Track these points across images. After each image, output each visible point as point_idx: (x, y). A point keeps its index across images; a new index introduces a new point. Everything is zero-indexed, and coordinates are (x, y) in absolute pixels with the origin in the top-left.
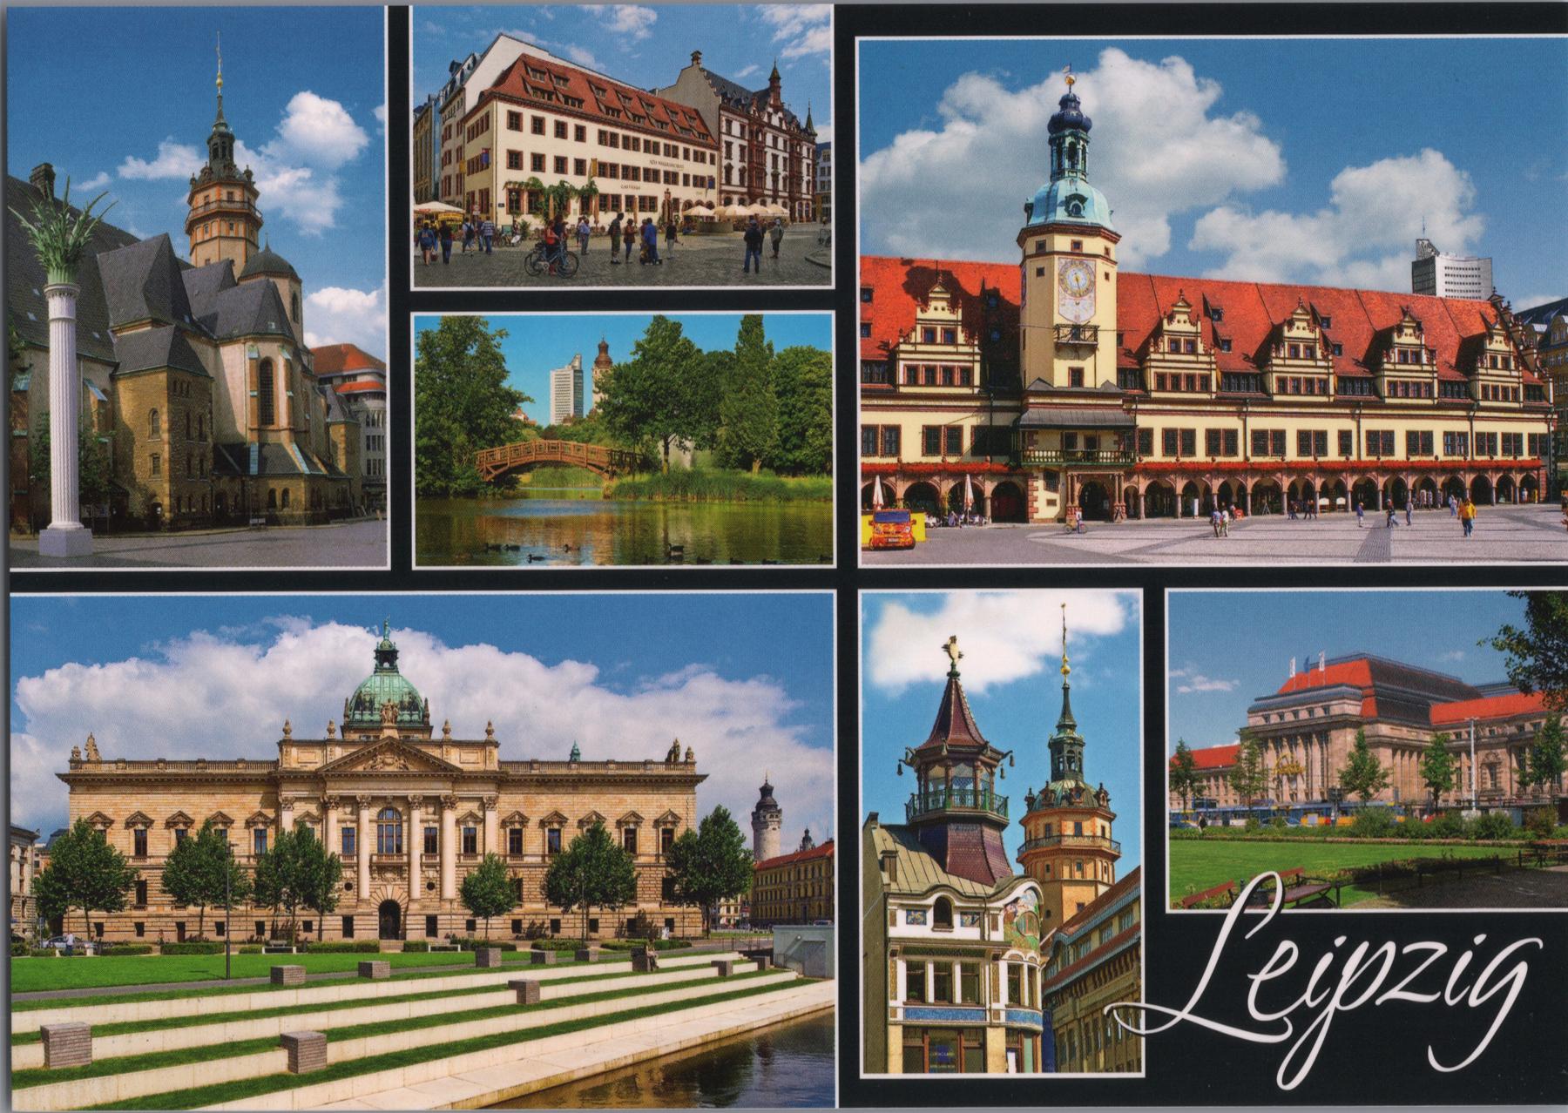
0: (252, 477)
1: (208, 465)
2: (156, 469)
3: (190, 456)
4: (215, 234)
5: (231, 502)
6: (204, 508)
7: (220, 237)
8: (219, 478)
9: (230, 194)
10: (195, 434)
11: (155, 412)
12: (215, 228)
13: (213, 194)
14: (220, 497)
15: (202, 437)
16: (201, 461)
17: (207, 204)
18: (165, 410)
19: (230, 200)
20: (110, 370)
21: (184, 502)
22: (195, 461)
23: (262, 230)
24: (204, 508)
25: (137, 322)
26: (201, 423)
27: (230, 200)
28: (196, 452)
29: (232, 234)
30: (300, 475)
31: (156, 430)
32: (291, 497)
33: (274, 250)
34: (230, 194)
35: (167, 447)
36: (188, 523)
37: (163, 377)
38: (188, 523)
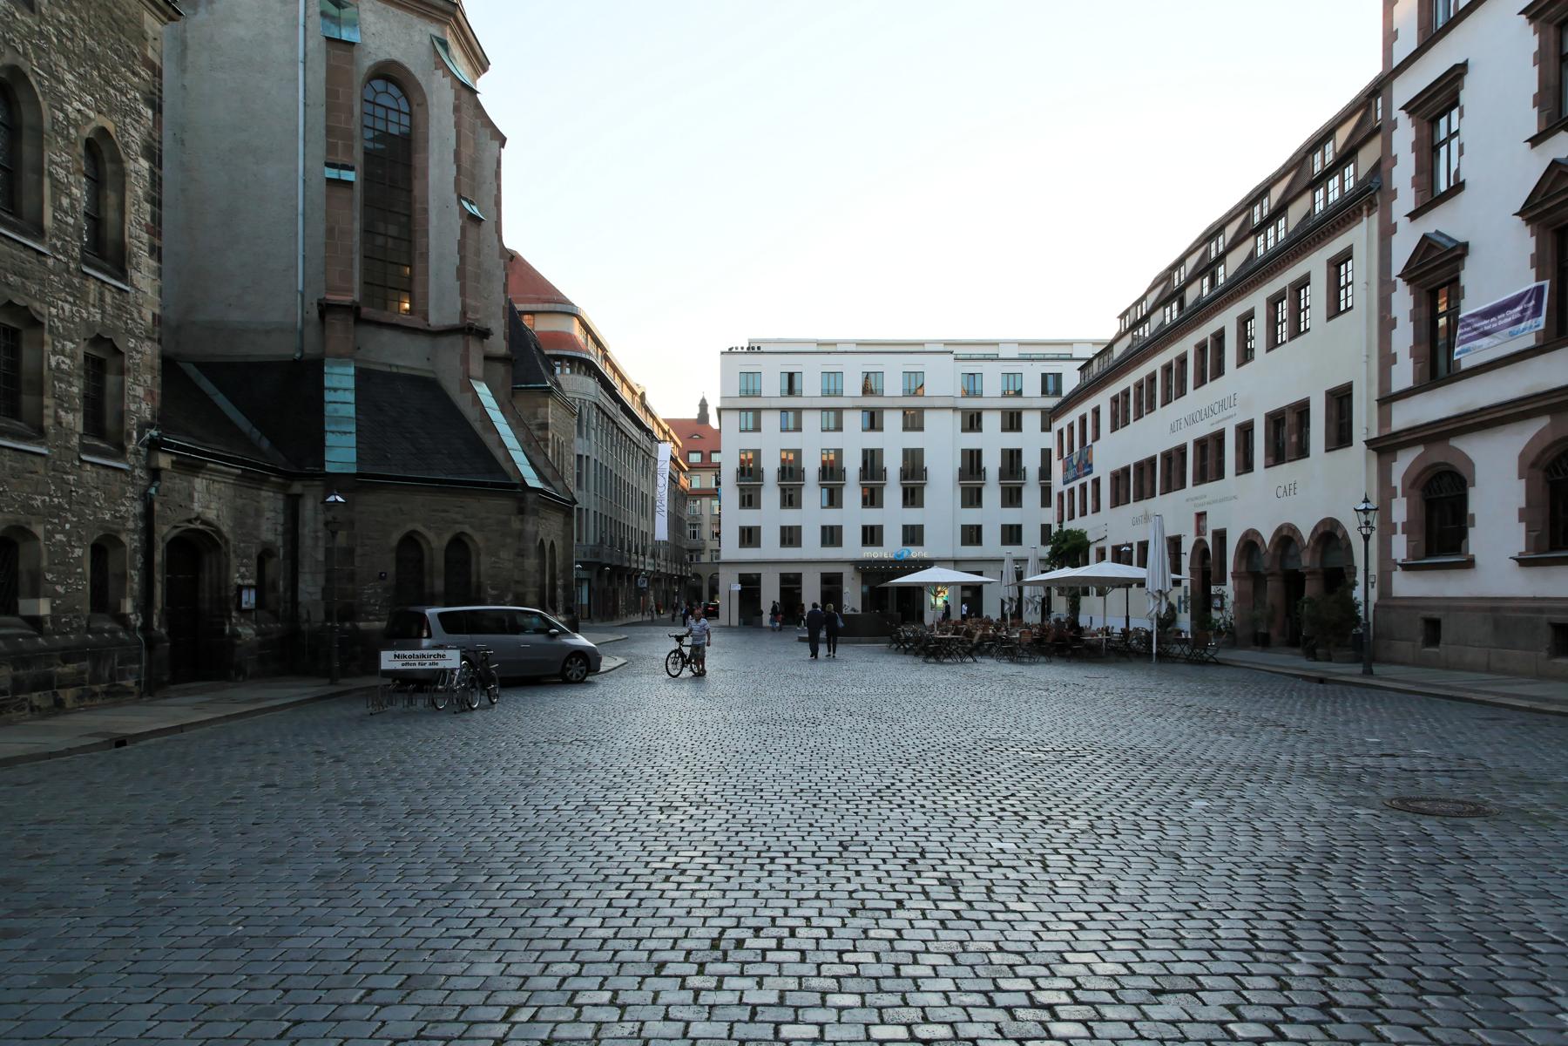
0: (336, 482)
5: (241, 574)
8: (189, 466)
14: (195, 548)
15: (107, 251)
24: (102, 599)
30: (514, 488)
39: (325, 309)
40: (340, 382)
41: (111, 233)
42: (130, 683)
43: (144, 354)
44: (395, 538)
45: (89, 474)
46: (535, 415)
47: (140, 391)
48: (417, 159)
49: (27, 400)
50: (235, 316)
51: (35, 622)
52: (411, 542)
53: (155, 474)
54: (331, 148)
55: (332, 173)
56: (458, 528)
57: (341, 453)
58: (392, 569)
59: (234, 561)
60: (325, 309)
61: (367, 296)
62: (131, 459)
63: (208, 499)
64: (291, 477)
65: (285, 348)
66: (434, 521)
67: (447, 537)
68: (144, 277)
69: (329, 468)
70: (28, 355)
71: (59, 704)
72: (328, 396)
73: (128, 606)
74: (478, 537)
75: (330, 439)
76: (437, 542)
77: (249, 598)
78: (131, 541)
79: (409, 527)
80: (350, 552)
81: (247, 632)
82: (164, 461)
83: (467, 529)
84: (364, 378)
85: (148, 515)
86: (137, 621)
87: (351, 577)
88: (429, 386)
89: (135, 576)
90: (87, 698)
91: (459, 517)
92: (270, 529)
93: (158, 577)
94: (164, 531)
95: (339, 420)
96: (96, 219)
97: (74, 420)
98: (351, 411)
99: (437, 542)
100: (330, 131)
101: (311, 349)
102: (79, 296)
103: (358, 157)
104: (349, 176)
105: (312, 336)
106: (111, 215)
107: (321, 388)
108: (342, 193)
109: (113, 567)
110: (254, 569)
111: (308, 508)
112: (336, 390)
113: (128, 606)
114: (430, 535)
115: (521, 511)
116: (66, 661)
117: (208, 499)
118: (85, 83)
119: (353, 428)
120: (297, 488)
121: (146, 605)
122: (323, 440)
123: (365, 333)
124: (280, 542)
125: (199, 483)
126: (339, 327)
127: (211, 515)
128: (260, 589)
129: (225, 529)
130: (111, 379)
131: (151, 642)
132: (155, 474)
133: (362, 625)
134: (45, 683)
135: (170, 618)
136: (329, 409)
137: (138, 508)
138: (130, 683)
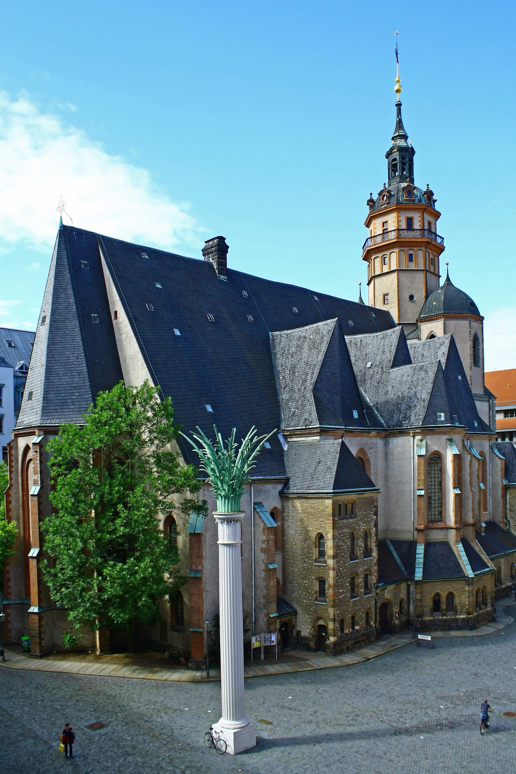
1: (373, 579)
2: (322, 592)
4: (394, 267)
6: (368, 623)
7: (398, 271)
10: (359, 552)
11: (321, 536)
12: (393, 259)
13: (392, 221)
16: (366, 576)
18: (330, 536)
20: (280, 487)
23: (443, 258)
24: (368, 623)
25: (307, 432)
31: (322, 554)
32: (457, 600)
35: (331, 573)
37: (329, 503)
40: (420, 549)
42: (373, 639)
44: (432, 595)
47: (374, 577)
49: (356, 589)
51: (357, 630)
52: (438, 595)
56: (449, 591)
59: (394, 605)
62: (372, 592)
63: (388, 594)
65: (409, 537)
66: (443, 589)
67: (446, 593)
69: (416, 579)
70: (356, 581)
71: (361, 646)
73: (372, 623)
74: (455, 592)
76: (444, 595)
78: (373, 610)
79: (436, 592)
80: (421, 600)
81: (397, 622)
83: (452, 591)
85: (376, 603)
86: (374, 626)
87: (421, 607)
88: (446, 544)
89: (373, 616)
91: (450, 588)
93: (378, 615)
94: (379, 605)
99: (444, 595)
107: (416, 548)
109: (370, 615)
110: (399, 606)
111: (412, 588)
112: (419, 554)
113: (372, 623)
114: (442, 593)
115: (468, 584)
116: (362, 637)
117: (388, 594)
119: (422, 566)
121: (375, 623)
122: (415, 570)
124: (405, 597)
127: (389, 597)
129: (392, 599)
130: (369, 577)
133: (424, 618)
136: (417, 560)
137: (374, 602)
138: (373, 639)
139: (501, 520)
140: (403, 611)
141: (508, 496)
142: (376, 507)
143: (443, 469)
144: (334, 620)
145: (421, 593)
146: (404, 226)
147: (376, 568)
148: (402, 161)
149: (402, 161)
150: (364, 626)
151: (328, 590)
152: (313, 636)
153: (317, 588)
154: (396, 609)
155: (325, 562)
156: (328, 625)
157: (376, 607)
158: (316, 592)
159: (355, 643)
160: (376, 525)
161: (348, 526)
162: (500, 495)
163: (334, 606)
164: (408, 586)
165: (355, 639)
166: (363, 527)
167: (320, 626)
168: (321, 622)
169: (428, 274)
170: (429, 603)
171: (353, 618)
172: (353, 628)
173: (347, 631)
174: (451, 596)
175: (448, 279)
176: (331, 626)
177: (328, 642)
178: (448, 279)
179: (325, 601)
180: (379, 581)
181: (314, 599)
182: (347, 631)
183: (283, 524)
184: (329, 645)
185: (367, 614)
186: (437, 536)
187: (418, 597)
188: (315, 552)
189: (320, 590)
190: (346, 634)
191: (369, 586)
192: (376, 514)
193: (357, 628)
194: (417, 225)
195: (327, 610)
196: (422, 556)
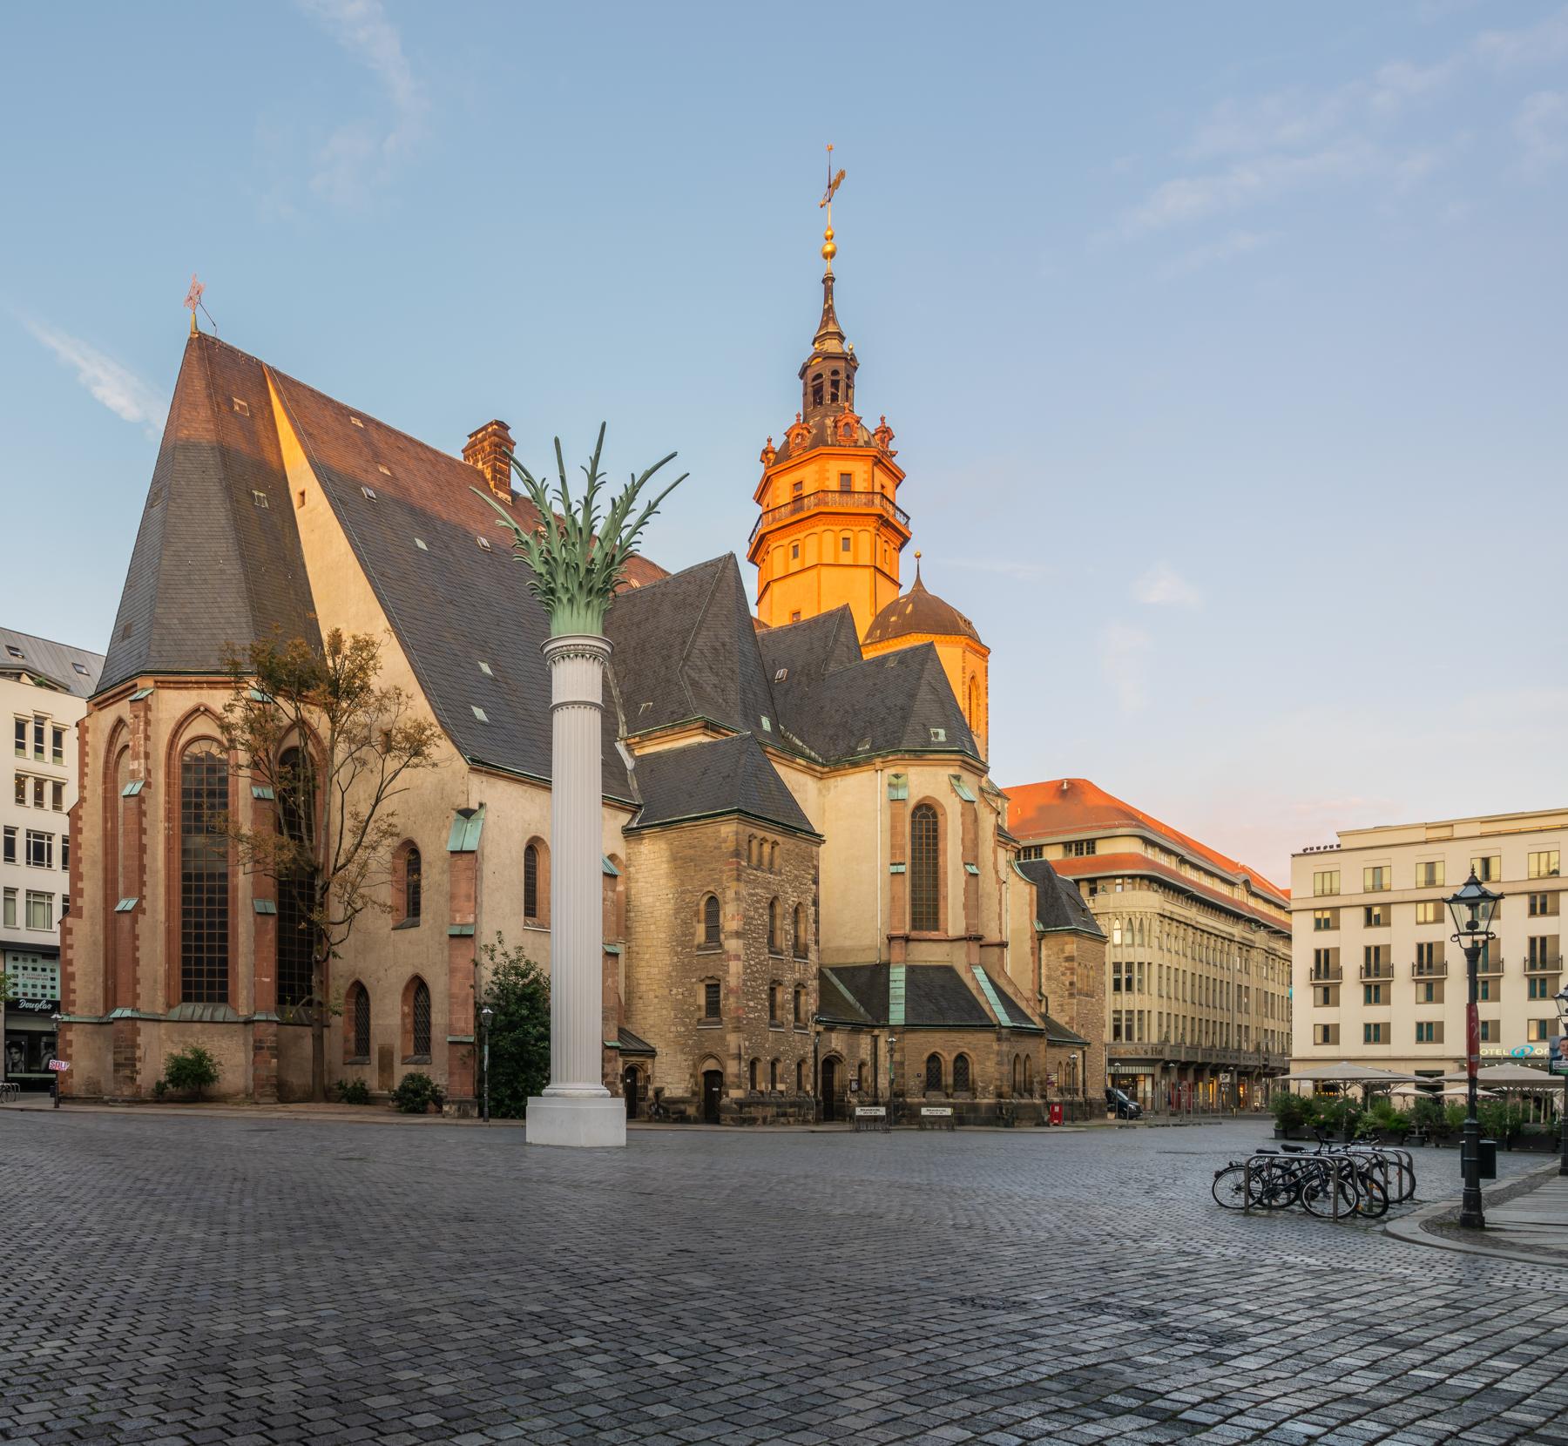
0: (893, 1030)
1: (810, 1003)
3: (774, 986)
6: (800, 1086)
8: (830, 1028)
9: (846, 477)
10: (784, 941)
14: (830, 1063)
15: (800, 951)
17: (798, 499)
19: (846, 490)
21: (762, 1069)
22: (784, 996)
24: (800, 1086)
26: (796, 923)
27: (846, 490)
28: (789, 978)
29: (846, 558)
30: (990, 1026)
31: (714, 931)
33: (932, 589)
34: (846, 477)
36: (770, 1111)
38: (770, 1111)
39: (891, 939)
40: (898, 975)
41: (802, 940)
43: (813, 984)
44: (925, 1056)
45: (797, 1037)
46: (1063, 951)
48: (941, 846)
49: (779, 1013)
50: (848, 943)
52: (934, 1058)
53: (818, 1033)
54: (893, 855)
55: (894, 869)
57: (897, 1014)
58: (924, 1072)
60: (891, 939)
61: (914, 927)
63: (837, 1042)
64: (874, 1027)
68: (812, 956)
72: (892, 985)
73: (808, 1088)
75: (892, 1008)
77: (854, 1086)
78: (811, 1062)
80: (902, 1063)
82: (820, 1028)
84: (912, 970)
85: (816, 1051)
87: (903, 1076)
90: (797, 1122)
92: (865, 1052)
94: (821, 1057)
95: (896, 997)
96: (796, 937)
97: (791, 1017)
98: (903, 992)
100: (893, 847)
101: (884, 958)
102: (793, 970)
103: (908, 861)
104: (902, 869)
105: (884, 950)
106: (802, 934)
107: (888, 980)
108: (899, 878)
113: (808, 1088)
117: (837, 1042)
118: (795, 889)
120: (876, 1032)
121: (815, 1088)
123: (912, 945)
125: (833, 1035)
126: (898, 947)
128: (859, 1082)
130: (803, 998)
131: (818, 1103)
132: (818, 1033)
134: (785, 1115)
135: (824, 1093)
139: (1028, 994)
140: (864, 1085)
141: (1044, 952)
142: (816, 868)
143: (941, 830)
144: (739, 1057)
145: (902, 1049)
146: (834, 484)
147: (815, 983)
148: (828, 381)
149: (828, 381)
150: (795, 1087)
151: (726, 998)
152: (694, 1094)
153: (702, 1001)
154: (852, 1075)
155: (721, 946)
156: (724, 1068)
157: (816, 1057)
158: (699, 1008)
159: (778, 1115)
160: (816, 903)
161: (767, 886)
162: (1028, 950)
163: (737, 1029)
164: (875, 1038)
165: (779, 1105)
166: (793, 899)
167: (708, 1074)
168: (711, 1065)
169: (879, 576)
170: (916, 1069)
171: (773, 1064)
172: (774, 1087)
173: (762, 1086)
174: (961, 1058)
175: (918, 582)
176: (732, 1068)
177: (725, 1100)
178: (918, 582)
179: (720, 1023)
180: (820, 1011)
181: (694, 1021)
182: (762, 1086)
183: (628, 889)
184: (728, 1109)
185: (799, 1066)
186: (930, 954)
187: (897, 1057)
188: (701, 929)
189: (708, 1003)
190: (762, 1092)
191: (802, 1015)
192: (816, 882)
193: (781, 1087)
194: (859, 484)
195: (723, 1038)
196: (903, 984)
